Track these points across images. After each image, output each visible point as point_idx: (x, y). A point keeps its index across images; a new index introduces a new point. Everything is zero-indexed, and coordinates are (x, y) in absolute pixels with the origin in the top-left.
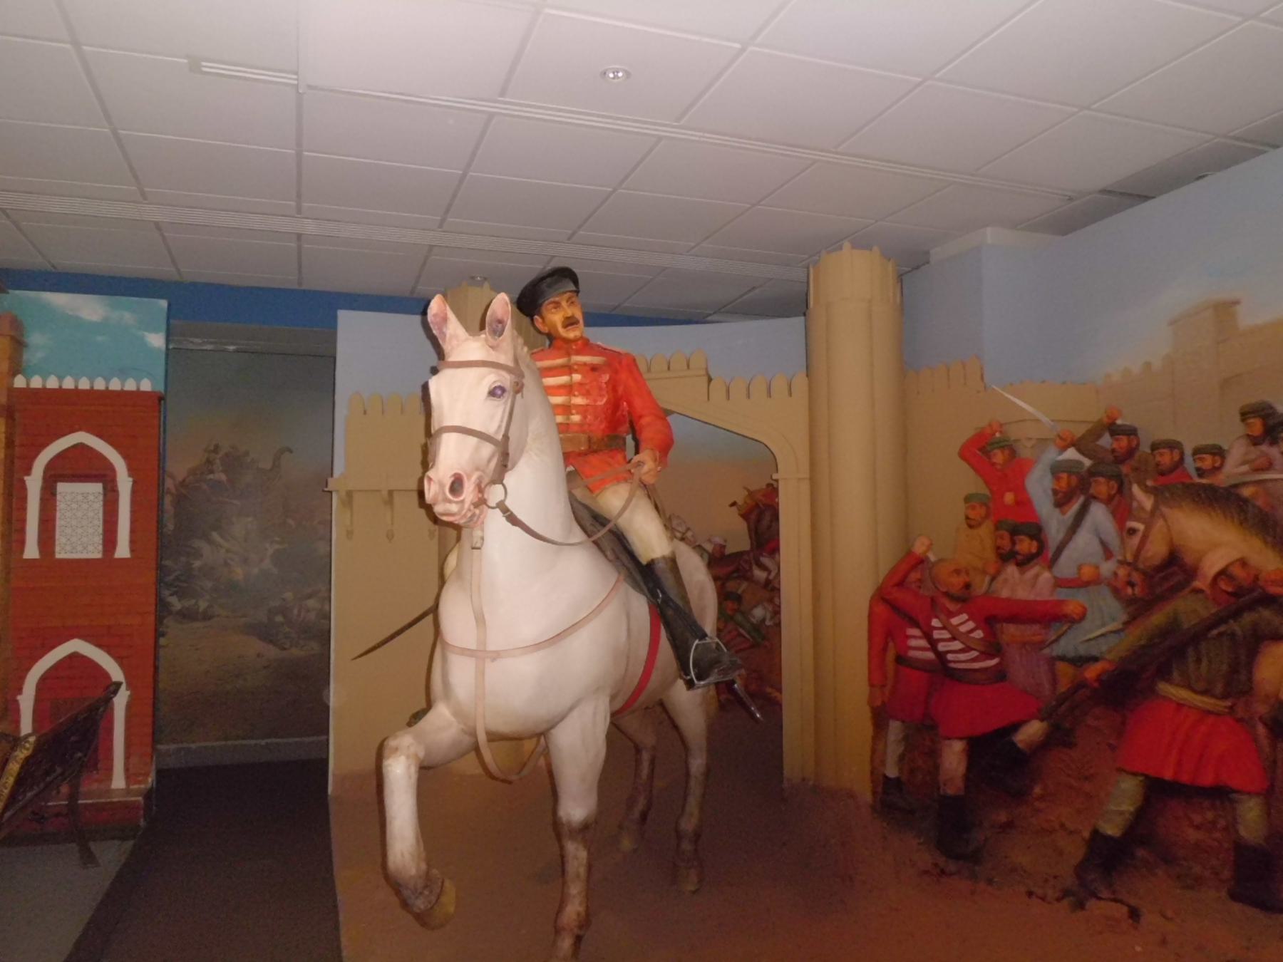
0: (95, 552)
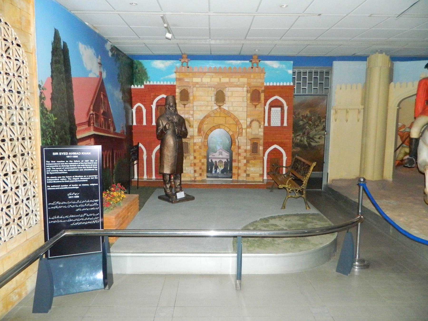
0: (279, 125)
